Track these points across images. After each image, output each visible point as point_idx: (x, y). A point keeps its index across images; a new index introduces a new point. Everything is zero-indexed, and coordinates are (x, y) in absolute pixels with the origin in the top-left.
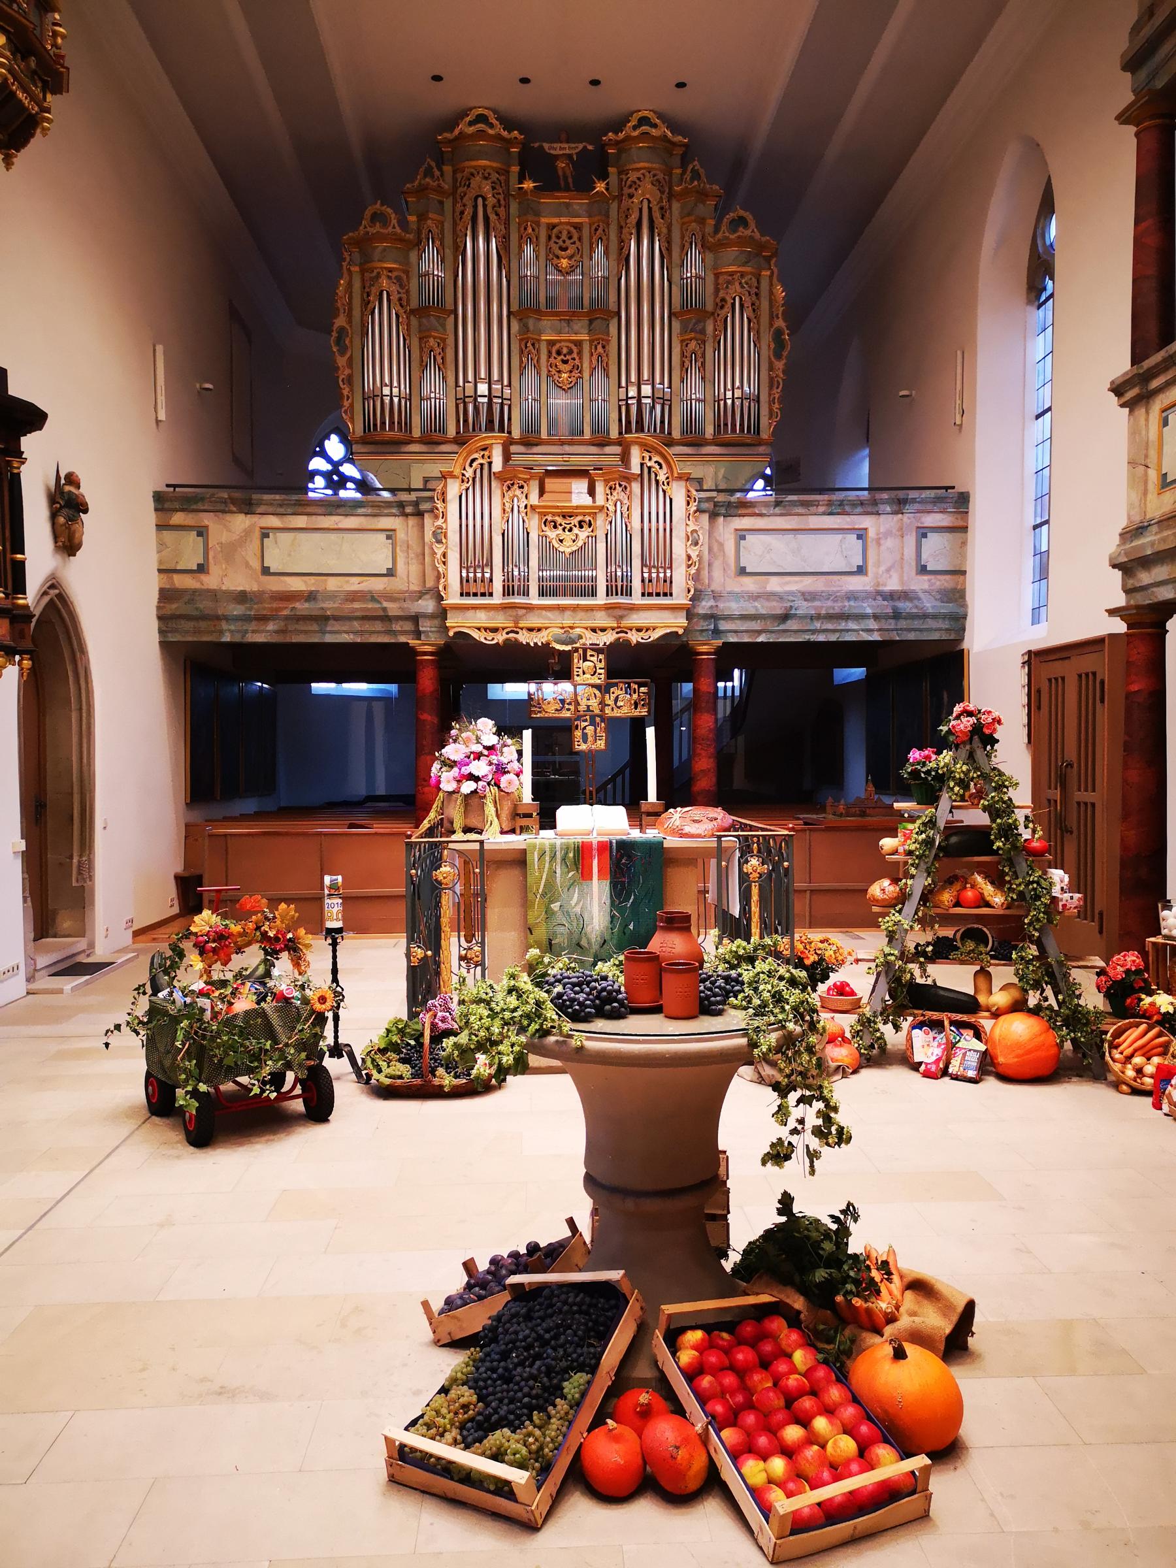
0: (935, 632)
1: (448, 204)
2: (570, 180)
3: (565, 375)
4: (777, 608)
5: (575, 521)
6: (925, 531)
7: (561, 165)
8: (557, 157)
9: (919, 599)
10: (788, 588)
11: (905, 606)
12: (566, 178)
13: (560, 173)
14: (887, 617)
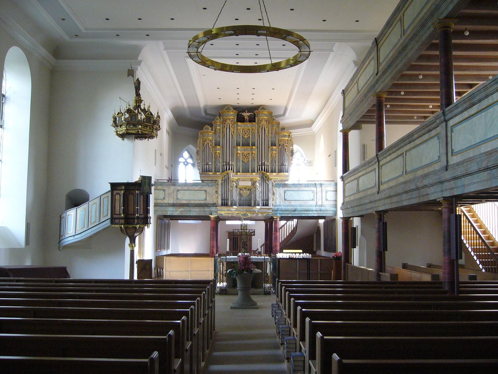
0: (329, 214)
1: (221, 125)
2: (248, 120)
3: (245, 160)
4: (293, 208)
5: (247, 189)
6: (327, 191)
7: (245, 117)
8: (245, 116)
9: (326, 206)
10: (296, 204)
11: (322, 208)
12: (247, 120)
13: (245, 119)
14: (318, 211)
